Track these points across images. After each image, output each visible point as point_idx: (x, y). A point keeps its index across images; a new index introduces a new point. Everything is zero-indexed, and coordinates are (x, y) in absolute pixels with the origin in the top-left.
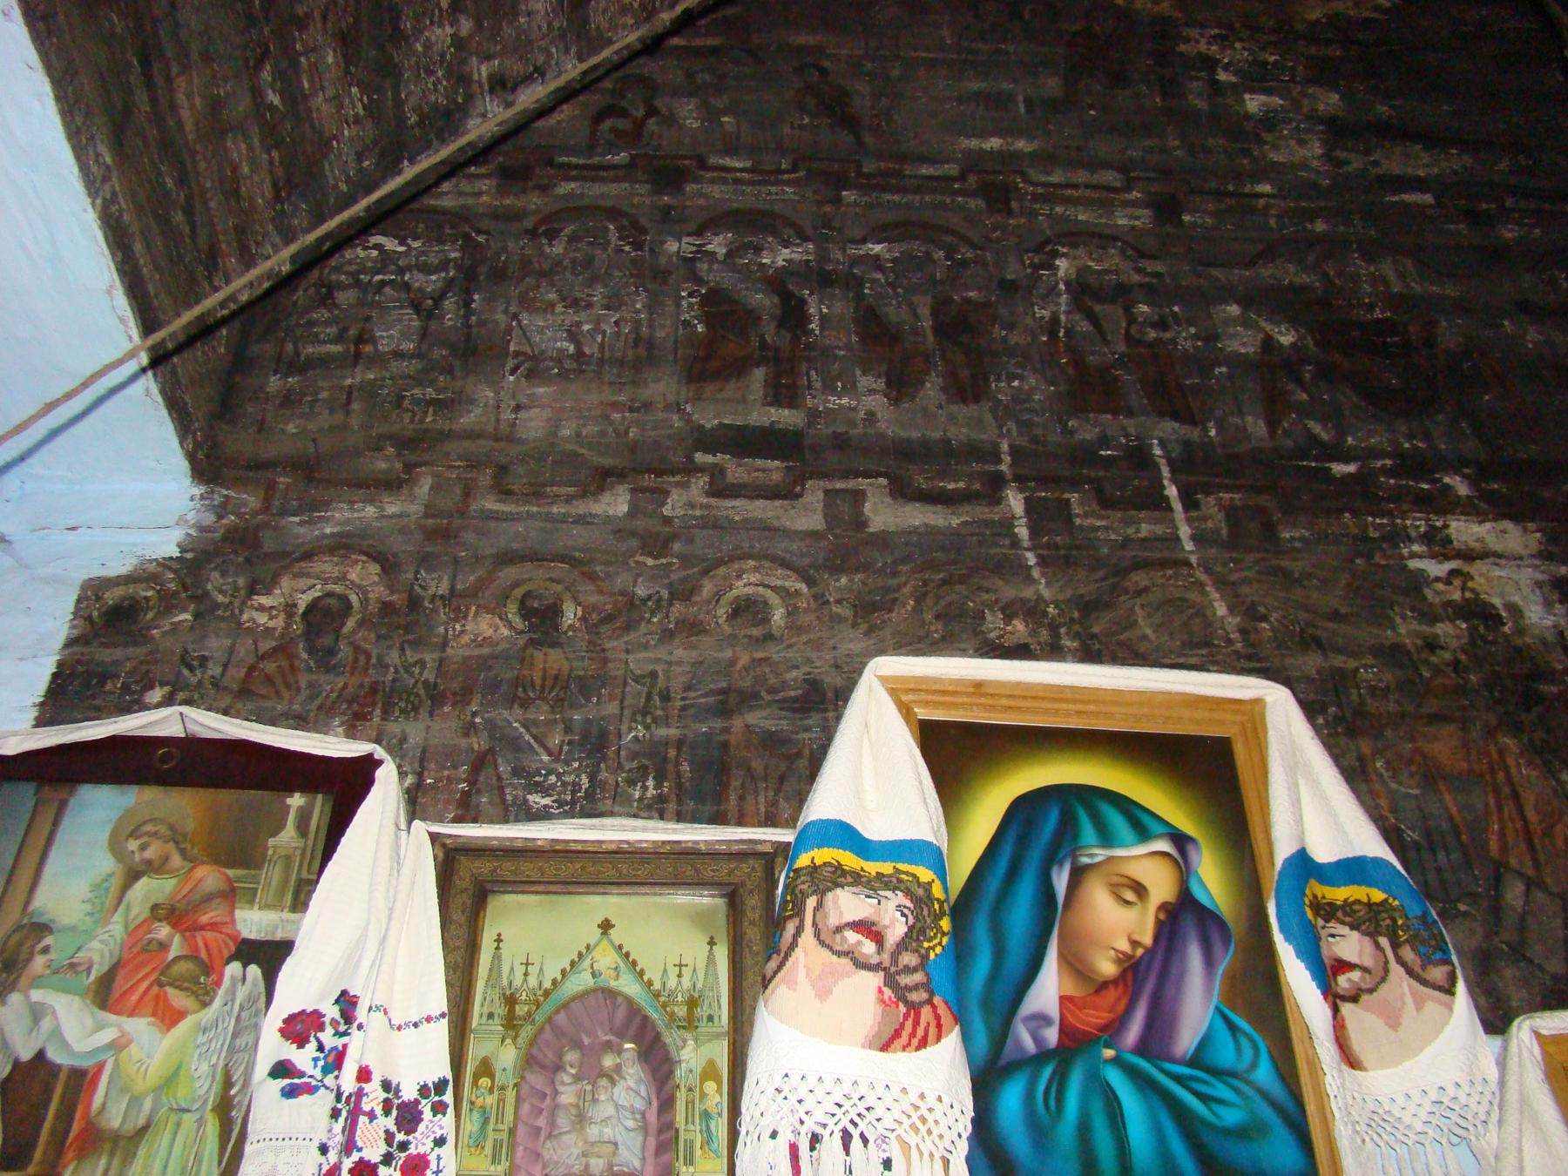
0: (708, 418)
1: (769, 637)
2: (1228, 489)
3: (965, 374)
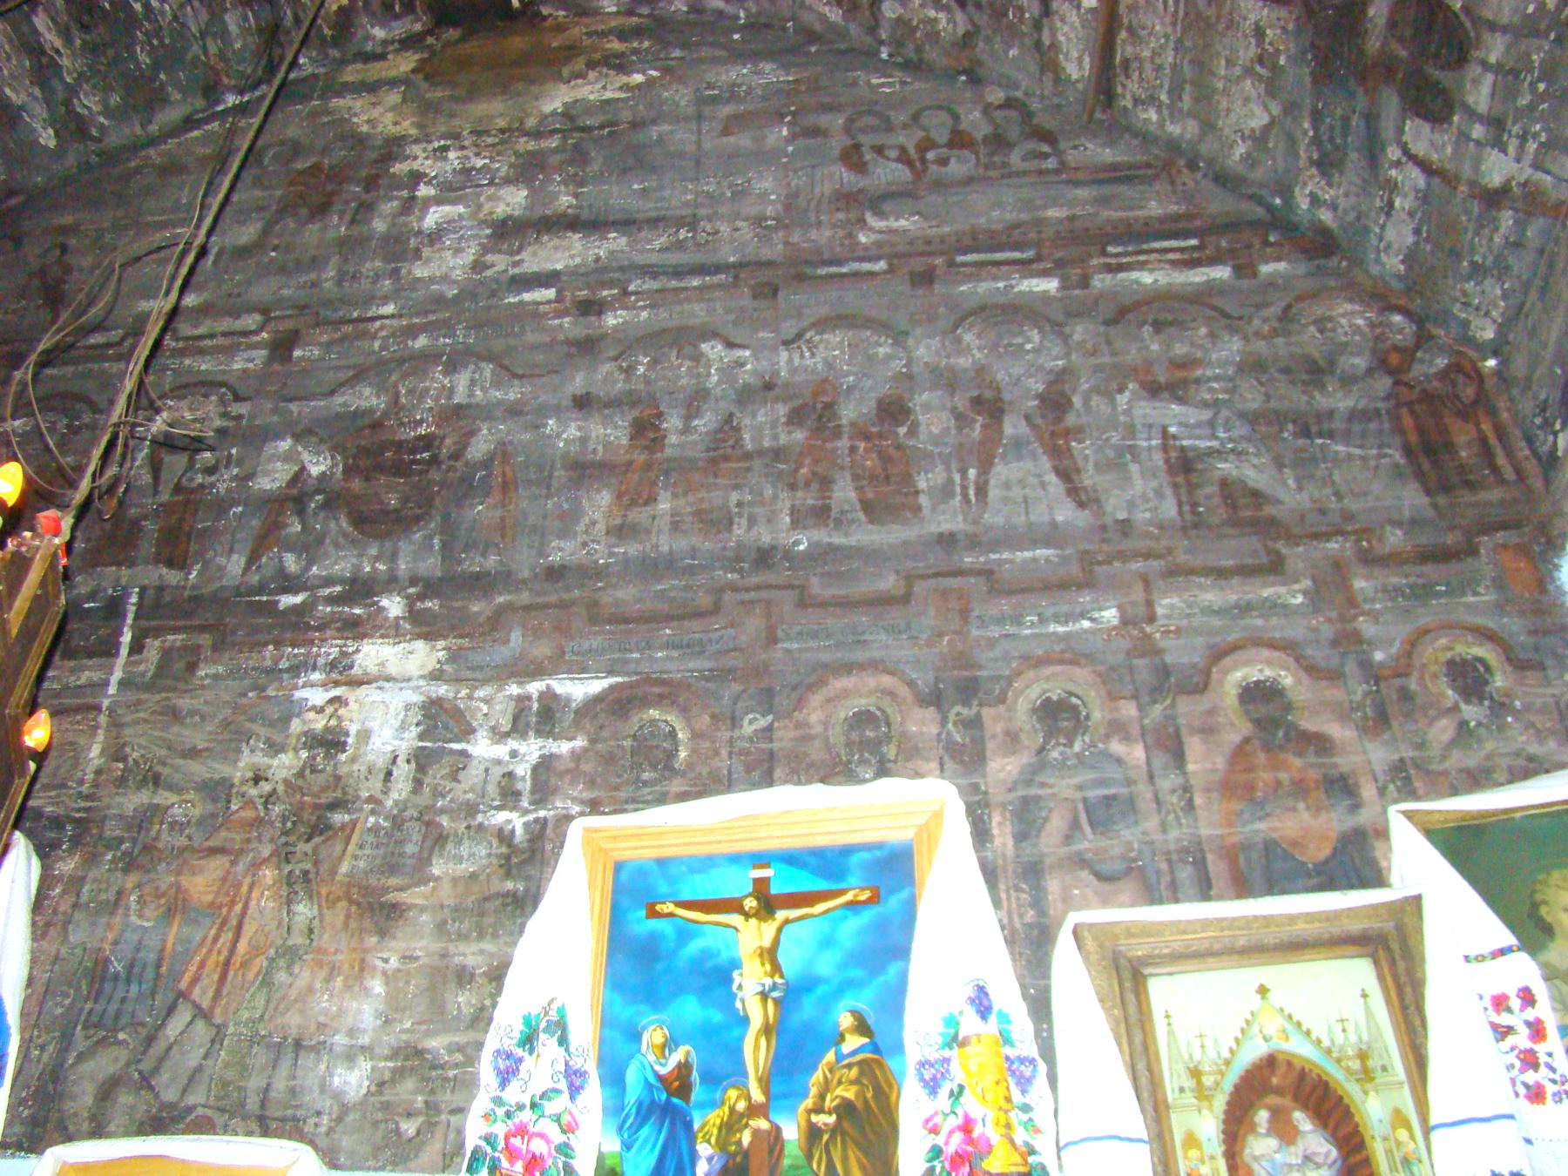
2: (176, 630)
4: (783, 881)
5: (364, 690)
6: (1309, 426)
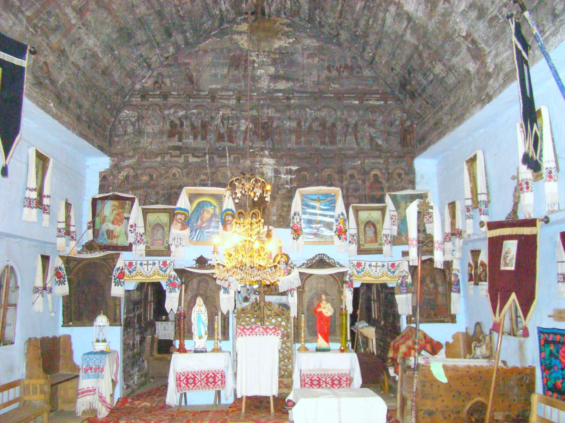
3: (204, 135)
4: (321, 197)
5: (265, 166)
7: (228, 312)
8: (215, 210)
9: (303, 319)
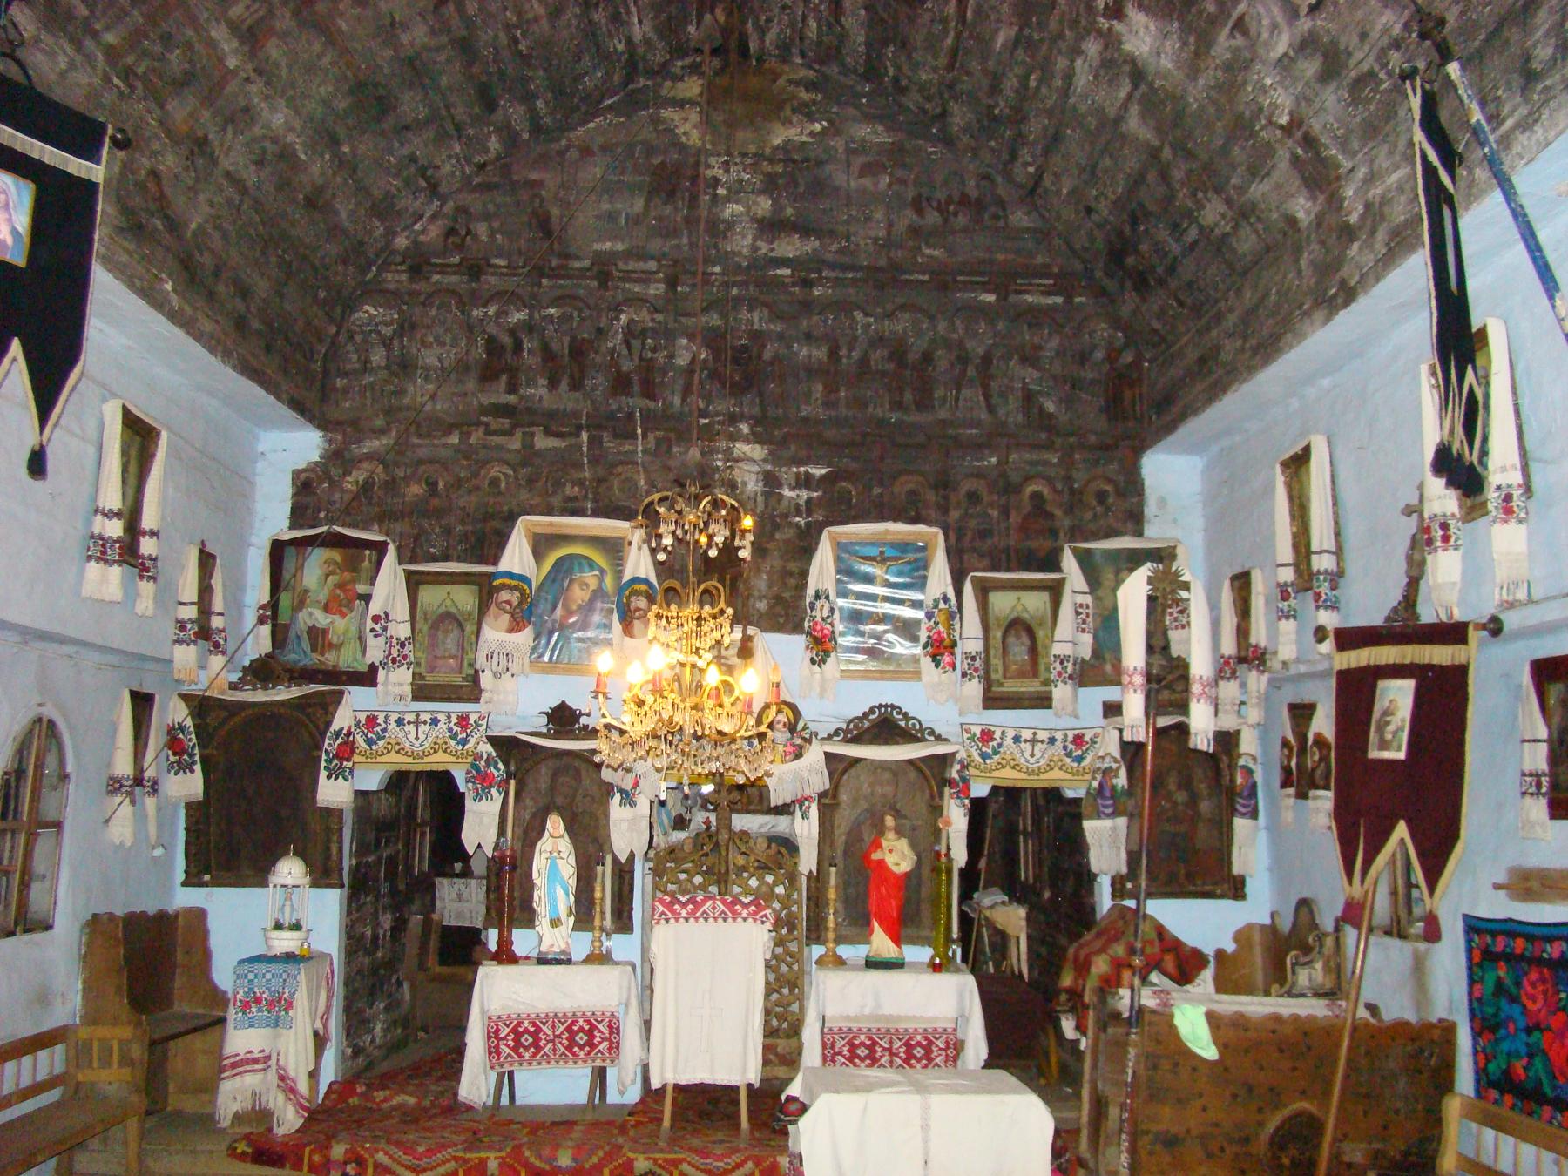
0: (487, 399)
1: (500, 493)
3: (577, 376)
4: (889, 552)
6: (1075, 384)
7: (632, 855)
8: (601, 579)
9: (833, 881)
